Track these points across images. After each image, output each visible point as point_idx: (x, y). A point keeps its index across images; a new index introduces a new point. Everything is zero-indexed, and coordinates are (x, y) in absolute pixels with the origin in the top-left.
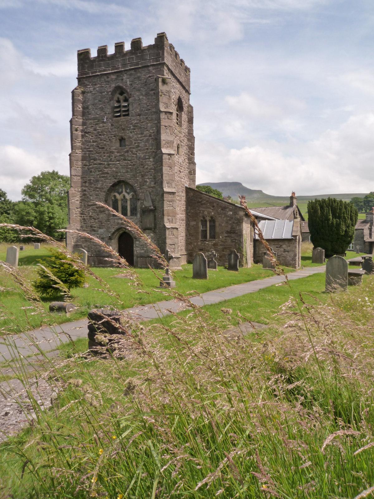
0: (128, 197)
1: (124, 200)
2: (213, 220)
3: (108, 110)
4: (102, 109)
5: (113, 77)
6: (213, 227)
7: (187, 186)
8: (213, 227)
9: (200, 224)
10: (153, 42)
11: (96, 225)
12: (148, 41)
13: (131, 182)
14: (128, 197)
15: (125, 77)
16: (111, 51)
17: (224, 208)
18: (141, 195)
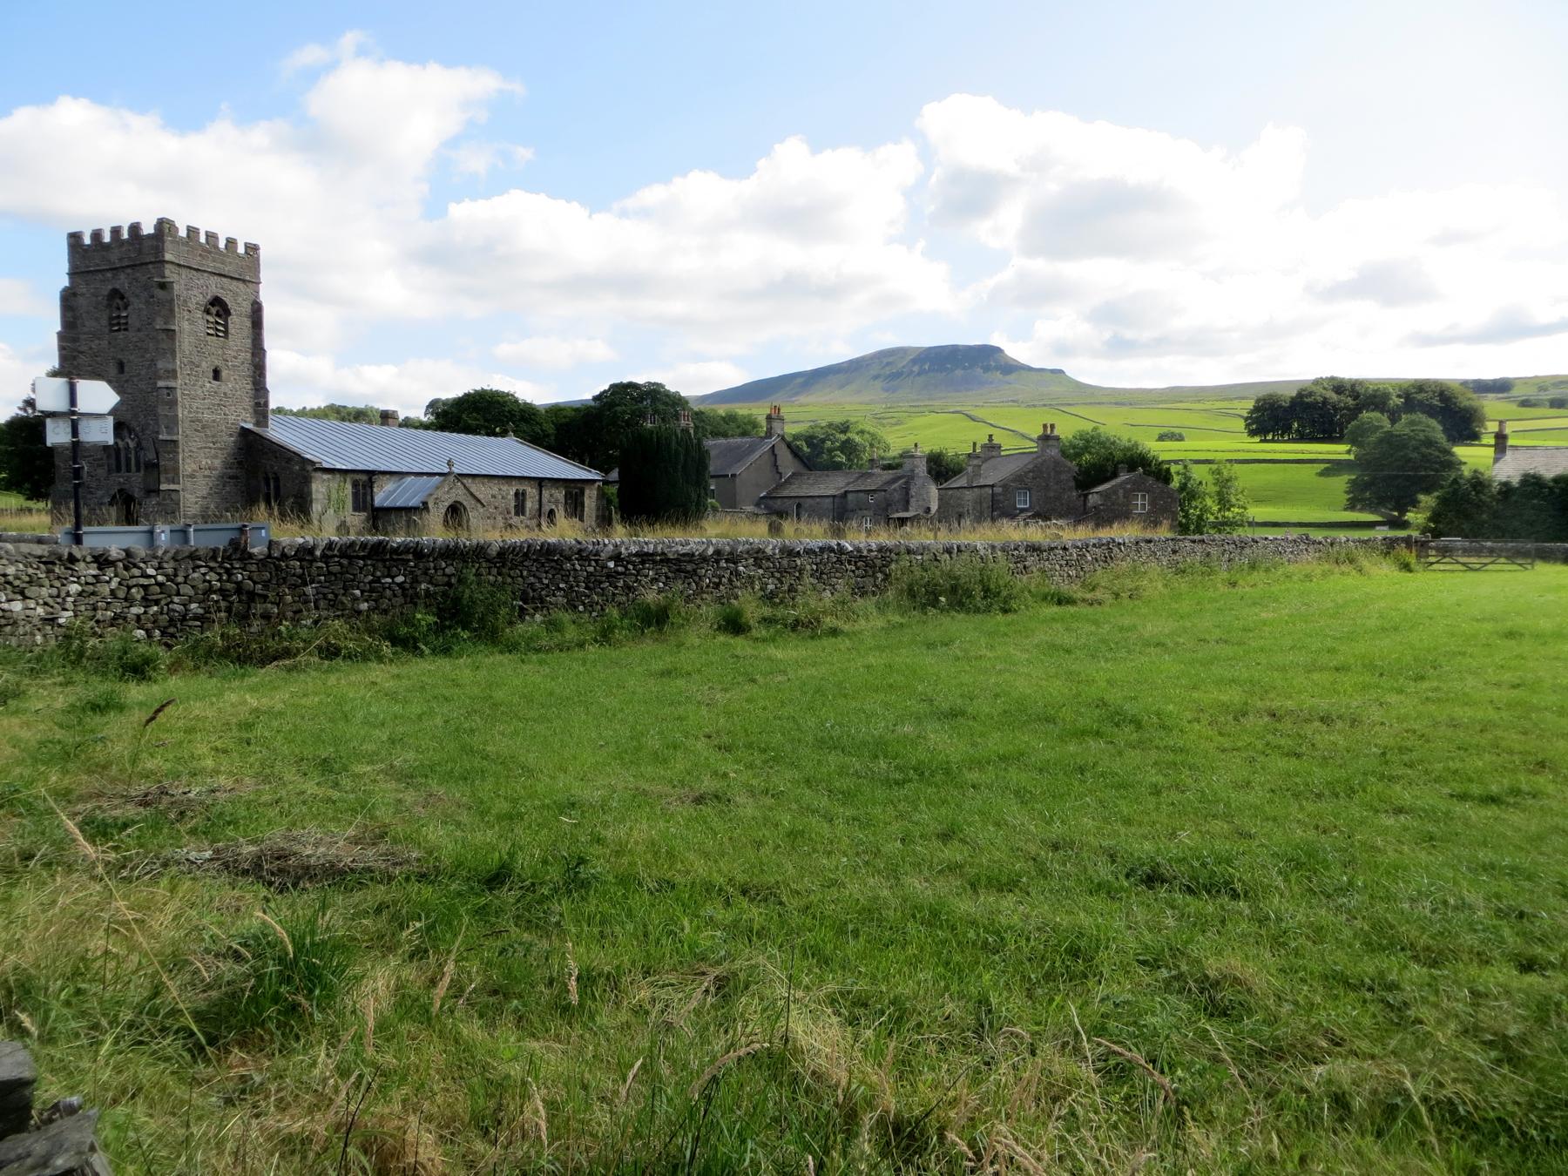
0: (132, 445)
1: (127, 448)
2: (277, 480)
3: (104, 322)
4: (97, 319)
5: (109, 275)
6: (277, 488)
7: (249, 426)
8: (277, 488)
9: (262, 484)
10: (152, 231)
11: (94, 485)
12: (148, 229)
13: (134, 424)
14: (132, 445)
15: (122, 276)
16: (107, 238)
17: (289, 460)
18: (144, 443)
